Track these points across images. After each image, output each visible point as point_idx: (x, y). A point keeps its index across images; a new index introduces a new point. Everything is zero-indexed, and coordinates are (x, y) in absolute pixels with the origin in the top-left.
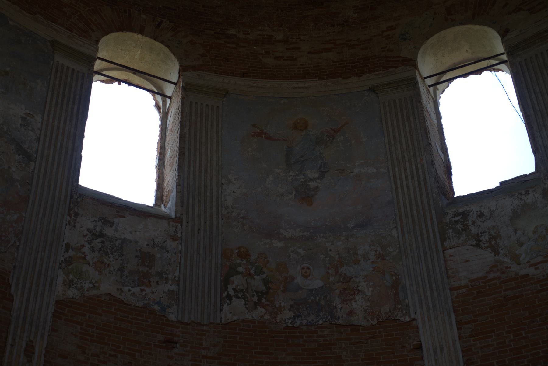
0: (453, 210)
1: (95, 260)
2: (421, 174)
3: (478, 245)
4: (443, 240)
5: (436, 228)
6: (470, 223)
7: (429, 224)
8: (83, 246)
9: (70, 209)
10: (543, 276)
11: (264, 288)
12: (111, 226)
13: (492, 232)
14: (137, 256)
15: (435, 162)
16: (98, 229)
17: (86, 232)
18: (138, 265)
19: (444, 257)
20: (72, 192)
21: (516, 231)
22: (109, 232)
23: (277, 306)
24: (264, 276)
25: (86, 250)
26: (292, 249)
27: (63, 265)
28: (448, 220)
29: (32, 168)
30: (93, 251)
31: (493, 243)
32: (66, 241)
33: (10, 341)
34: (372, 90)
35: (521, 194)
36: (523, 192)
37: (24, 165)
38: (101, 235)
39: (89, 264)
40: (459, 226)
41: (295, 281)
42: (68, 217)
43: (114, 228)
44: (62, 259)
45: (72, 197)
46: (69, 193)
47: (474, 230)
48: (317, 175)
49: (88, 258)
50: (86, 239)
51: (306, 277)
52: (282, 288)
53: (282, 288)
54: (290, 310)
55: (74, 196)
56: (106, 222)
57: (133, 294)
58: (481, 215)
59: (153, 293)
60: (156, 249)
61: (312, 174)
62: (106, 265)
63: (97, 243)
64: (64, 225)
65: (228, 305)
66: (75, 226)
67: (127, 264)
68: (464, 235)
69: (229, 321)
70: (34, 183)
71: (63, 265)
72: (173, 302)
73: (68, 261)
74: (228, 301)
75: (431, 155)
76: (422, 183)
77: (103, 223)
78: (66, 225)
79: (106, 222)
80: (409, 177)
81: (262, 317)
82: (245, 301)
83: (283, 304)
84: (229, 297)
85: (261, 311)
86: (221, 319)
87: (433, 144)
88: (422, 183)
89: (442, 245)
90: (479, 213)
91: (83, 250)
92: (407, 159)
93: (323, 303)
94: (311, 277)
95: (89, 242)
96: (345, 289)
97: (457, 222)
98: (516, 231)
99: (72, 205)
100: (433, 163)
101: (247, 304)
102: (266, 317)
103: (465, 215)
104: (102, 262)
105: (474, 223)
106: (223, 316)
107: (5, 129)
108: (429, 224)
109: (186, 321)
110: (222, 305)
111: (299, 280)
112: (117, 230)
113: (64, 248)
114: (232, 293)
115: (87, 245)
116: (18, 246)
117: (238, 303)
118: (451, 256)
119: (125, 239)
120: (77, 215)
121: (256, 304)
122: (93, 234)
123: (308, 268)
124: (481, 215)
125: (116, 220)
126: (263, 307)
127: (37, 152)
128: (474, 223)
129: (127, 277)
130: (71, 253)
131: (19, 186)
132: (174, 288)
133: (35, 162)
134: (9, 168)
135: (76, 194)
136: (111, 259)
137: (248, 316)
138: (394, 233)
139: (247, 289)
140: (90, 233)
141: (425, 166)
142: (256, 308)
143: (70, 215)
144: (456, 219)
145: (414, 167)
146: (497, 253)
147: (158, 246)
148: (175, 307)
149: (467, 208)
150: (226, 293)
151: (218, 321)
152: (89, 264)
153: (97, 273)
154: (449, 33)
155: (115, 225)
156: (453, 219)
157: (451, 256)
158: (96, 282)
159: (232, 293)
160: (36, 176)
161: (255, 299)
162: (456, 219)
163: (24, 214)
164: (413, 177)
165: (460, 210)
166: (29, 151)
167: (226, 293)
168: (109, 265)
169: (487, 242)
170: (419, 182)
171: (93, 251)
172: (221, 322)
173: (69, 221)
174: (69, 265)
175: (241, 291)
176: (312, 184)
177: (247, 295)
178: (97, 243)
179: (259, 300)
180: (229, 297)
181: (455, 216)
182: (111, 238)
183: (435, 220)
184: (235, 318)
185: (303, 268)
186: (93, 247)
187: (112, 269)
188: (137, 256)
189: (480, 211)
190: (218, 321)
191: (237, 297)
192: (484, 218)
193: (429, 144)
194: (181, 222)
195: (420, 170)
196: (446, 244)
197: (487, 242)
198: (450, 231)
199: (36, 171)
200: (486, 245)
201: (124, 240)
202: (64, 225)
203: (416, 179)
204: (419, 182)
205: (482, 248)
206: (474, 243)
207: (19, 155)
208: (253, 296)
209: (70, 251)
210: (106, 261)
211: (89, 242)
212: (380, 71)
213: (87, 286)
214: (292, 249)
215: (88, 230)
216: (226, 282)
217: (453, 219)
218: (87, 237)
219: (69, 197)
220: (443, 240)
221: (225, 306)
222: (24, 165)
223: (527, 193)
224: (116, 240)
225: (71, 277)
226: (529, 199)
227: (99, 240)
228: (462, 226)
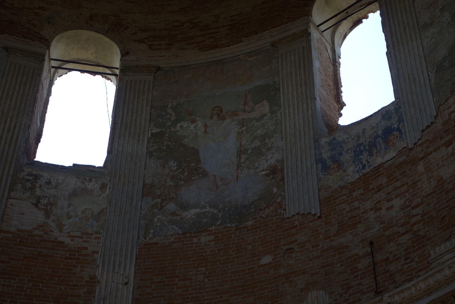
0: (29, 170)
2: (16, 131)
3: (36, 205)
4: (11, 190)
5: (10, 178)
6: (38, 185)
7: (6, 173)
10: (75, 248)
13: (51, 200)
15: (32, 127)
19: (6, 203)
21: (69, 205)
28: (21, 176)
31: (48, 208)
34: (6, 49)
35: (85, 179)
36: (88, 179)
47: (38, 192)
58: (49, 183)
68: (29, 193)
75: (31, 120)
76: (14, 139)
80: (6, 130)
87: (36, 112)
88: (14, 139)
89: (9, 193)
90: (48, 181)
92: (10, 115)
97: (28, 180)
98: (69, 205)
100: (29, 127)
103: (37, 177)
105: (41, 186)
108: (6, 173)
118: (12, 205)
124: (49, 183)
128: (41, 186)
141: (23, 126)
144: (29, 178)
145: (13, 124)
146: (48, 217)
149: (41, 173)
154: (85, 34)
156: (26, 177)
157: (12, 205)
162: (29, 178)
164: (9, 131)
165: (34, 172)
169: (44, 205)
170: (12, 137)
181: (28, 175)
183: (11, 172)
189: (50, 180)
192: (50, 186)
193: (33, 112)
195: (17, 129)
196: (12, 194)
197: (44, 205)
198: (20, 185)
200: (42, 207)
203: (10, 134)
204: (12, 137)
205: (38, 209)
206: (34, 202)
212: (19, 37)
217: (26, 177)
220: (11, 190)
223: (90, 180)
226: (90, 186)
228: (30, 185)
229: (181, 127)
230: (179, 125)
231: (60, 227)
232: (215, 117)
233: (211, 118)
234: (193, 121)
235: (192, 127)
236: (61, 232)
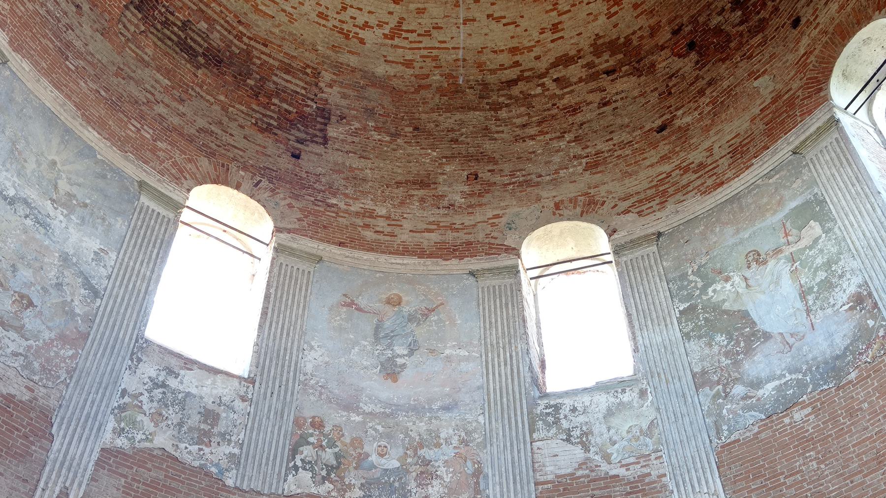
0: (545, 402)
1: (153, 410)
4: (532, 431)
5: (526, 418)
6: (562, 416)
7: (519, 413)
8: (141, 394)
9: (133, 354)
11: (335, 462)
12: (176, 378)
13: (584, 428)
14: (199, 413)
16: (161, 379)
17: (147, 380)
18: (200, 422)
19: (532, 449)
20: (138, 335)
22: (173, 383)
23: (347, 483)
24: (337, 450)
25: (144, 398)
26: (371, 425)
27: (116, 411)
28: (539, 412)
29: (98, 305)
30: (152, 401)
32: (123, 387)
35: (617, 392)
36: (620, 390)
37: (89, 301)
38: (164, 385)
39: (145, 414)
40: (550, 419)
41: (370, 459)
42: (130, 362)
43: (179, 380)
44: (116, 404)
45: (137, 341)
46: (135, 337)
47: (565, 424)
49: (144, 407)
50: (146, 387)
52: (354, 465)
53: (354, 465)
54: (360, 489)
55: (140, 340)
56: (170, 372)
57: (190, 453)
58: (574, 410)
59: (212, 453)
60: (222, 408)
62: (164, 418)
63: (158, 393)
64: (124, 369)
65: (293, 476)
66: (135, 372)
67: (188, 419)
68: (555, 429)
69: (292, 493)
70: (97, 321)
71: (116, 411)
72: (233, 466)
73: (122, 408)
74: (294, 472)
77: (167, 373)
78: (126, 369)
79: (170, 372)
81: (329, 492)
82: (313, 474)
83: (353, 482)
84: (296, 468)
85: (328, 486)
86: (284, 490)
89: (531, 436)
90: (572, 408)
91: (141, 398)
93: (397, 484)
94: (387, 456)
95: (149, 391)
96: (422, 473)
97: (548, 414)
99: (135, 350)
101: (315, 478)
102: (333, 494)
103: (557, 408)
104: (160, 414)
105: (566, 417)
106: (286, 487)
107: (74, 260)
108: (519, 413)
109: (244, 488)
110: (286, 475)
112: (181, 383)
113: (119, 393)
114: (299, 463)
115: (146, 394)
116: (69, 384)
117: (305, 476)
118: (538, 448)
119: (189, 392)
120: (139, 360)
121: (324, 479)
122: (155, 383)
123: (386, 447)
124: (574, 410)
125: (182, 372)
126: (331, 482)
127: (105, 290)
128: (566, 417)
129: (185, 433)
130: (127, 399)
131: (80, 321)
132: (236, 451)
133: (102, 299)
134: (72, 300)
135: (142, 339)
136: (171, 412)
137: (314, 490)
138: (481, 419)
139: (316, 462)
140: (151, 381)
142: (324, 483)
143: (132, 360)
144: (548, 411)
147: (225, 405)
148: (235, 471)
149: (560, 401)
150: (293, 463)
151: (280, 492)
152: (145, 414)
153: (153, 424)
155: (180, 377)
156: (545, 411)
157: (538, 448)
158: (150, 434)
159: (299, 463)
160: (100, 313)
161: (324, 473)
162: (548, 411)
163: (80, 352)
165: (552, 403)
166: (97, 287)
167: (293, 463)
168: (167, 417)
169: (578, 437)
171: (152, 401)
172: (283, 493)
173: (129, 366)
174: (122, 412)
175: (310, 462)
177: (316, 468)
178: (158, 393)
179: (328, 474)
180: (296, 468)
181: (546, 407)
182: (174, 390)
183: (525, 410)
184: (299, 491)
185: (380, 446)
186: (152, 397)
187: (170, 423)
188: (199, 413)
189: (574, 406)
190: (280, 492)
191: (304, 469)
192: (577, 413)
196: (535, 436)
197: (578, 437)
198: (540, 422)
199: (101, 309)
200: (576, 441)
201: (188, 394)
202: (124, 369)
205: (572, 444)
206: (565, 437)
207: (85, 289)
208: (323, 469)
209: (126, 397)
210: (164, 413)
211: (149, 391)
213: (139, 437)
214: (371, 425)
215: (150, 378)
216: (294, 452)
217: (545, 411)
218: (147, 386)
219: (133, 341)
220: (532, 431)
221: (290, 476)
222: (89, 301)
223: (624, 391)
224: (179, 393)
225: (123, 425)
226: (626, 398)
227: (161, 390)
228: (553, 419)
229: (714, 291)
230: (710, 290)
231: (607, 458)
232: (754, 265)
233: (749, 267)
234: (727, 279)
235: (728, 286)
236: (610, 463)
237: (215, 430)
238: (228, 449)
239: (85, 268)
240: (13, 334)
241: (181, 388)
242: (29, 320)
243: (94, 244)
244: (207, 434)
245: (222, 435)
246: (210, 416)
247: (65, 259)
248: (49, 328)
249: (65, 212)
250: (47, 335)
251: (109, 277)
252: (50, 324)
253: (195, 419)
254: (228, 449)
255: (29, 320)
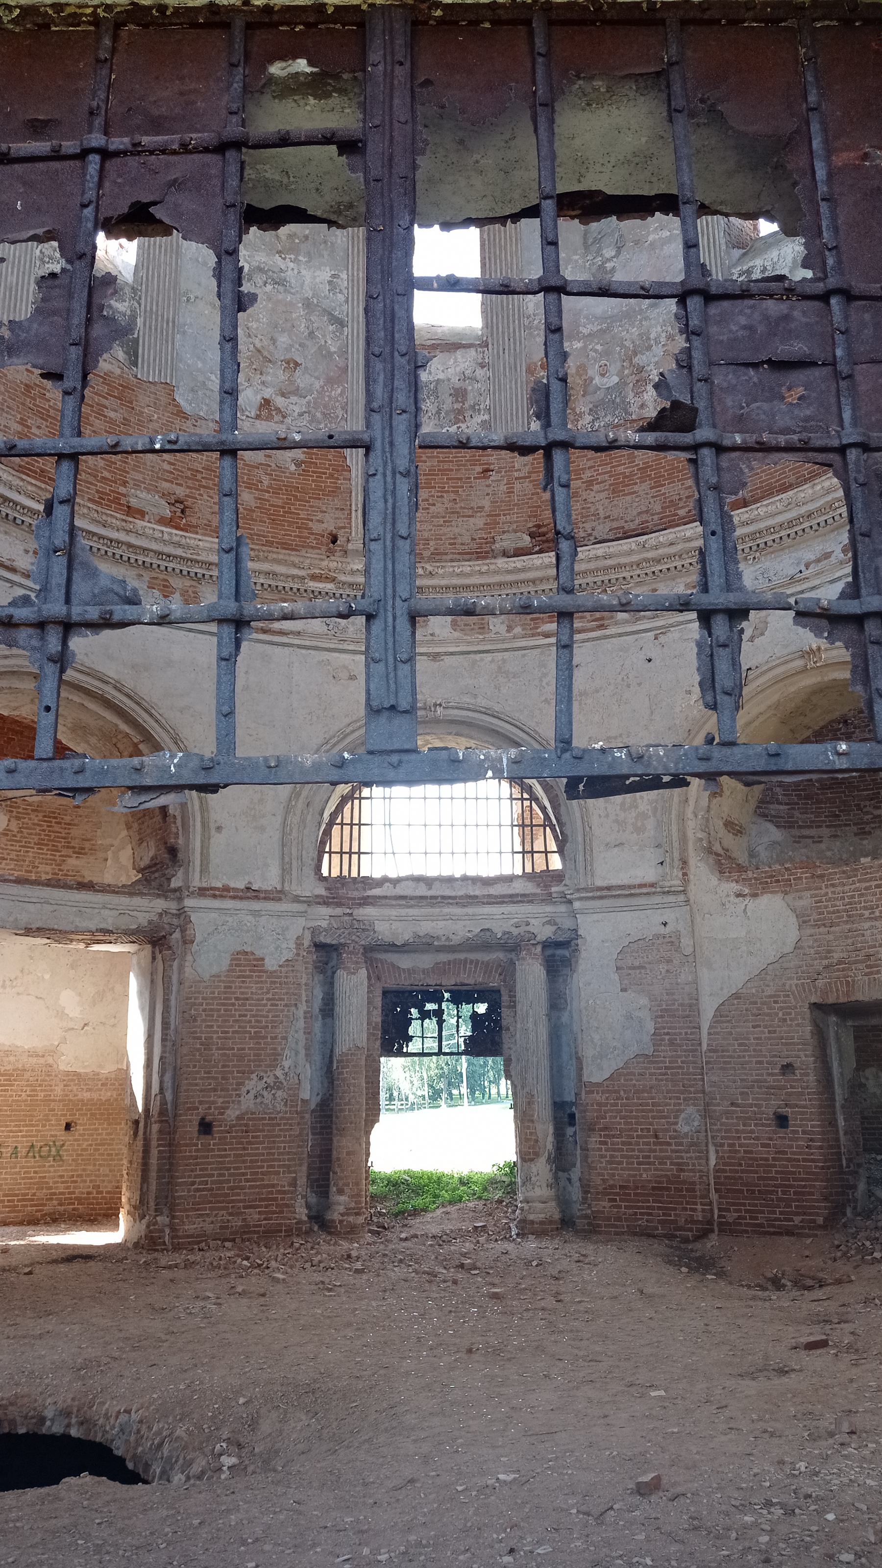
33: (354, 508)
48: (613, 253)
51: (603, 375)
61: (609, 253)
111: (597, 380)
132: (486, 417)
176: (609, 265)
194: (487, 346)
237: (466, 405)
238: (479, 419)
239: (326, 304)
240: (294, 399)
241: (431, 378)
242: (302, 380)
243: (325, 275)
244: (460, 412)
245: (473, 407)
246: (459, 394)
247: (308, 304)
248: (318, 378)
249: (292, 256)
250: (317, 385)
251: (347, 301)
252: (316, 374)
253: (448, 403)
254: (479, 419)
255: (302, 380)
